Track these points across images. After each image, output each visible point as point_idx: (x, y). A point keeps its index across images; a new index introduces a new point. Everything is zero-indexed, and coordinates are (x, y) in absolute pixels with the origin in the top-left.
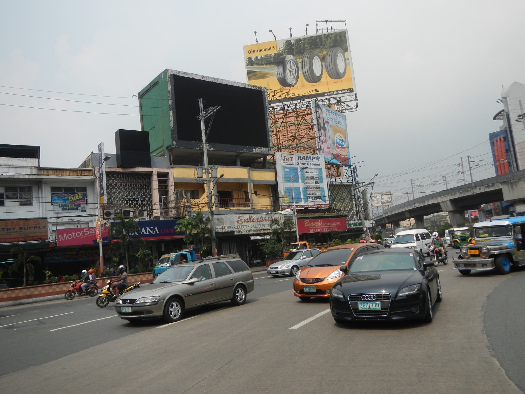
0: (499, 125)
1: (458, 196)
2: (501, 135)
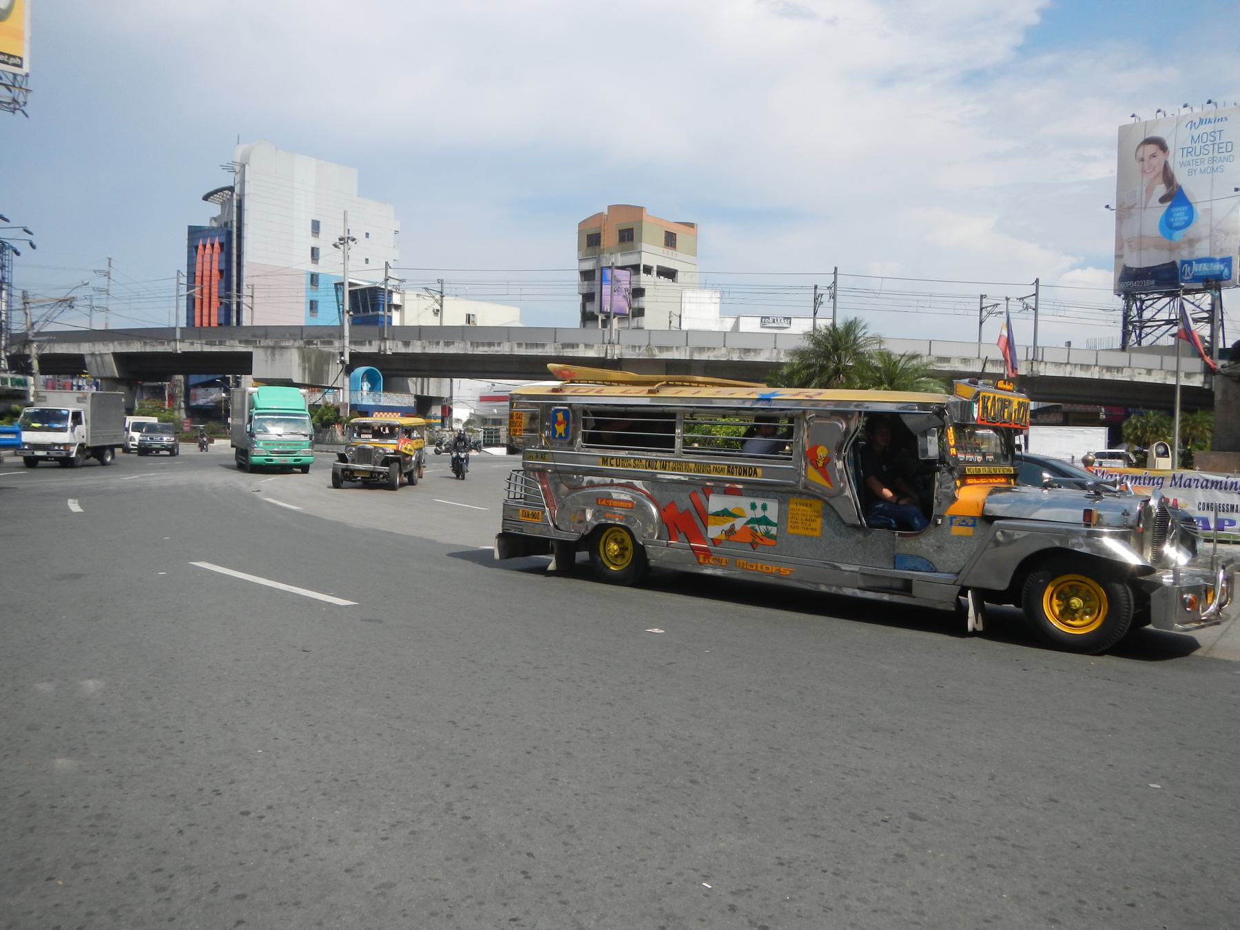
0: (208, 214)
1: (136, 347)
2: (215, 236)
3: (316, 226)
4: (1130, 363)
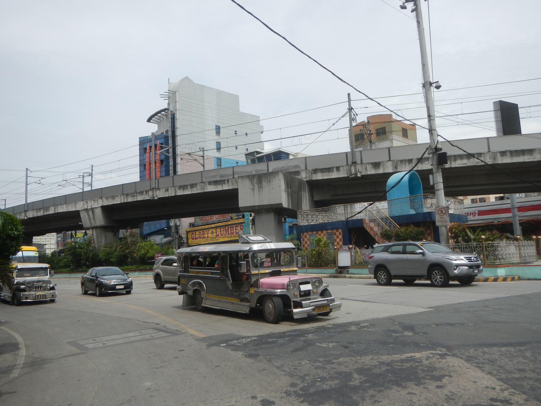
3: (218, 130)
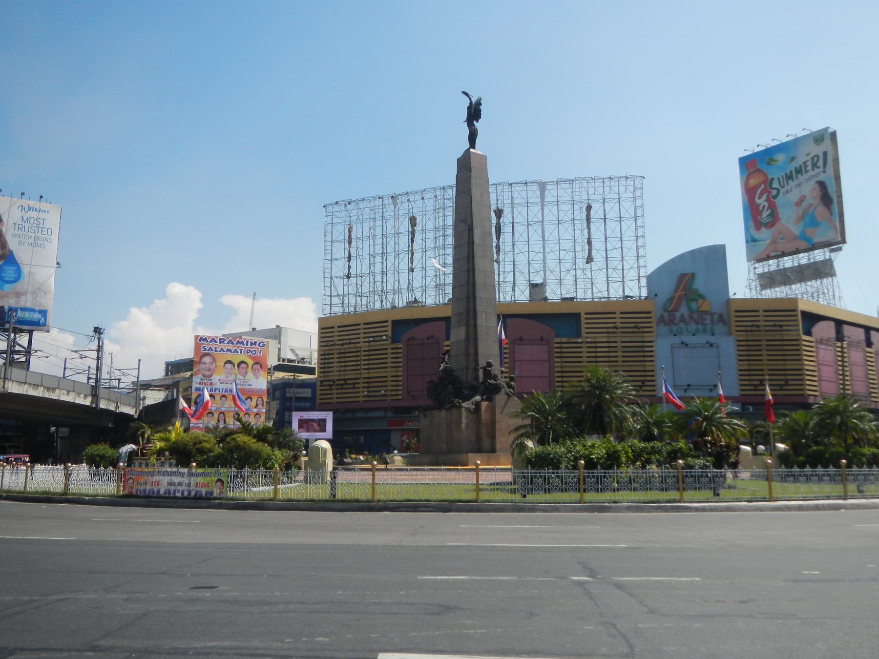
4: (42, 382)
